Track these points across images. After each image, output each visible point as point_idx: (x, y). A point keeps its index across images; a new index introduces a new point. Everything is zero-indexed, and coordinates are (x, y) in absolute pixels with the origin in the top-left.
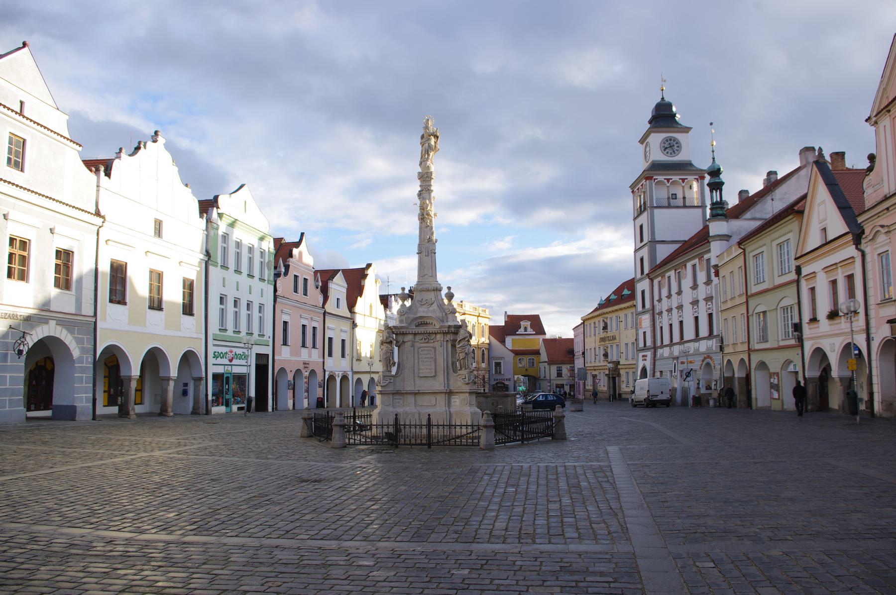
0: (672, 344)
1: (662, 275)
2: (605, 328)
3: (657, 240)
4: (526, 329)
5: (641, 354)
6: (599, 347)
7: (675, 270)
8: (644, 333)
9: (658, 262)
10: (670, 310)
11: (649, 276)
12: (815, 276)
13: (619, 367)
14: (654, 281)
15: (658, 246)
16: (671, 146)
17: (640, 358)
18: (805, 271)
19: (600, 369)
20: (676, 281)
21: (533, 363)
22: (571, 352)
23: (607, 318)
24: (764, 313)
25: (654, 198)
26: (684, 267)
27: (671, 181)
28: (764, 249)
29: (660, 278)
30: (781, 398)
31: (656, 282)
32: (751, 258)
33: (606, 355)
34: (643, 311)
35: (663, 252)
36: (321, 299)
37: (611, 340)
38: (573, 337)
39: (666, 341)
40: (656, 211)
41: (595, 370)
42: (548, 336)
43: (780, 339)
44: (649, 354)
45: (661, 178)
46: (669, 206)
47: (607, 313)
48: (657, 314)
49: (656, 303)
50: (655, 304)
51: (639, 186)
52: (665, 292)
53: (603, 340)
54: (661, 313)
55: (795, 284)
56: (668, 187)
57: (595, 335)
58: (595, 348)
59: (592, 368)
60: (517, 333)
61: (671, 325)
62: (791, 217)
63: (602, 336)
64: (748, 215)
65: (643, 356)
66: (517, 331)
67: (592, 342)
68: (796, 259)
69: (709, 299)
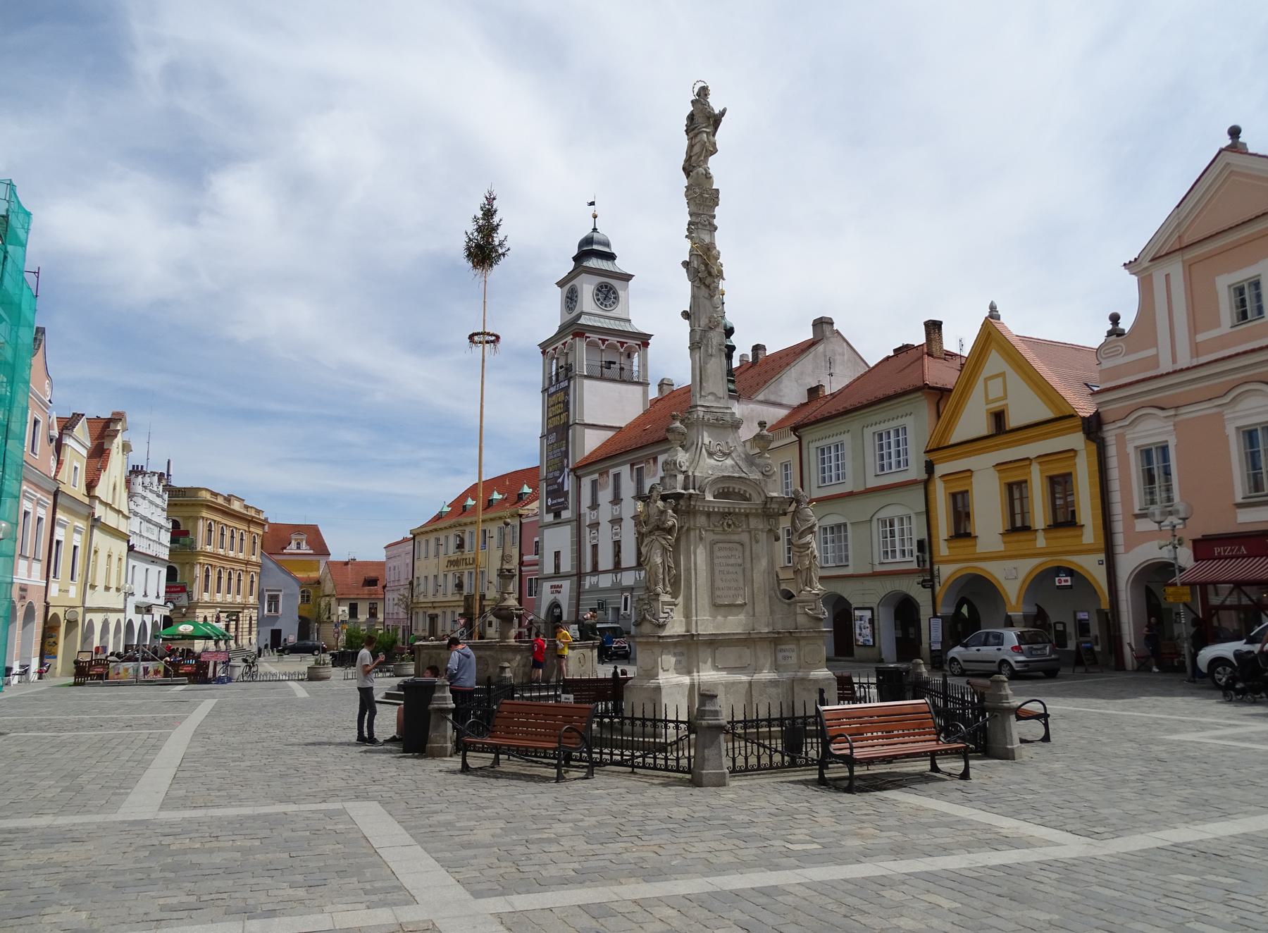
0: (617, 567)
1: (604, 473)
2: (460, 546)
3: (586, 422)
4: (299, 548)
6: (446, 575)
7: (632, 465)
8: (557, 554)
9: (587, 453)
11: (575, 473)
12: (971, 476)
14: (582, 479)
15: (588, 431)
16: (607, 294)
18: (940, 469)
19: (445, 607)
20: (632, 480)
21: (308, 596)
23: (463, 532)
24: (840, 527)
25: (585, 363)
26: (651, 461)
27: (606, 343)
28: (846, 438)
29: (596, 476)
30: (877, 645)
31: (586, 483)
32: (813, 452)
33: (459, 586)
34: (556, 522)
35: (592, 441)
36: (53, 465)
37: (470, 564)
38: (383, 559)
39: (606, 561)
40: (587, 382)
41: (434, 607)
42: (332, 558)
43: (876, 562)
44: (566, 585)
45: (594, 337)
46: (602, 378)
47: (466, 524)
48: (588, 526)
50: (582, 512)
51: (559, 344)
52: (605, 495)
53: (451, 563)
54: (595, 525)
55: (922, 486)
56: (602, 350)
57: (437, 555)
58: (436, 577)
59: (430, 605)
60: (285, 551)
61: (617, 545)
62: (919, 394)
63: (452, 559)
64: (761, 397)
65: (552, 587)
66: (285, 548)
67: (429, 567)
68: (926, 452)
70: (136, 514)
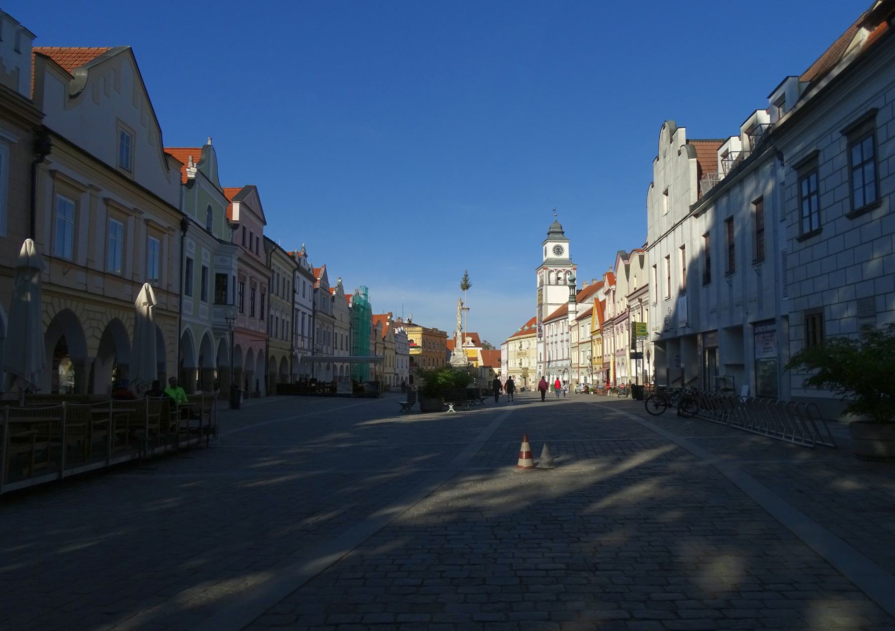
2: (521, 347)
5: (539, 365)
8: (541, 353)
9: (549, 315)
10: (552, 343)
13: (528, 371)
17: (538, 367)
22: (500, 360)
33: (521, 364)
49: (546, 338)
53: (519, 354)
54: (548, 344)
69: (567, 341)
70: (397, 341)
